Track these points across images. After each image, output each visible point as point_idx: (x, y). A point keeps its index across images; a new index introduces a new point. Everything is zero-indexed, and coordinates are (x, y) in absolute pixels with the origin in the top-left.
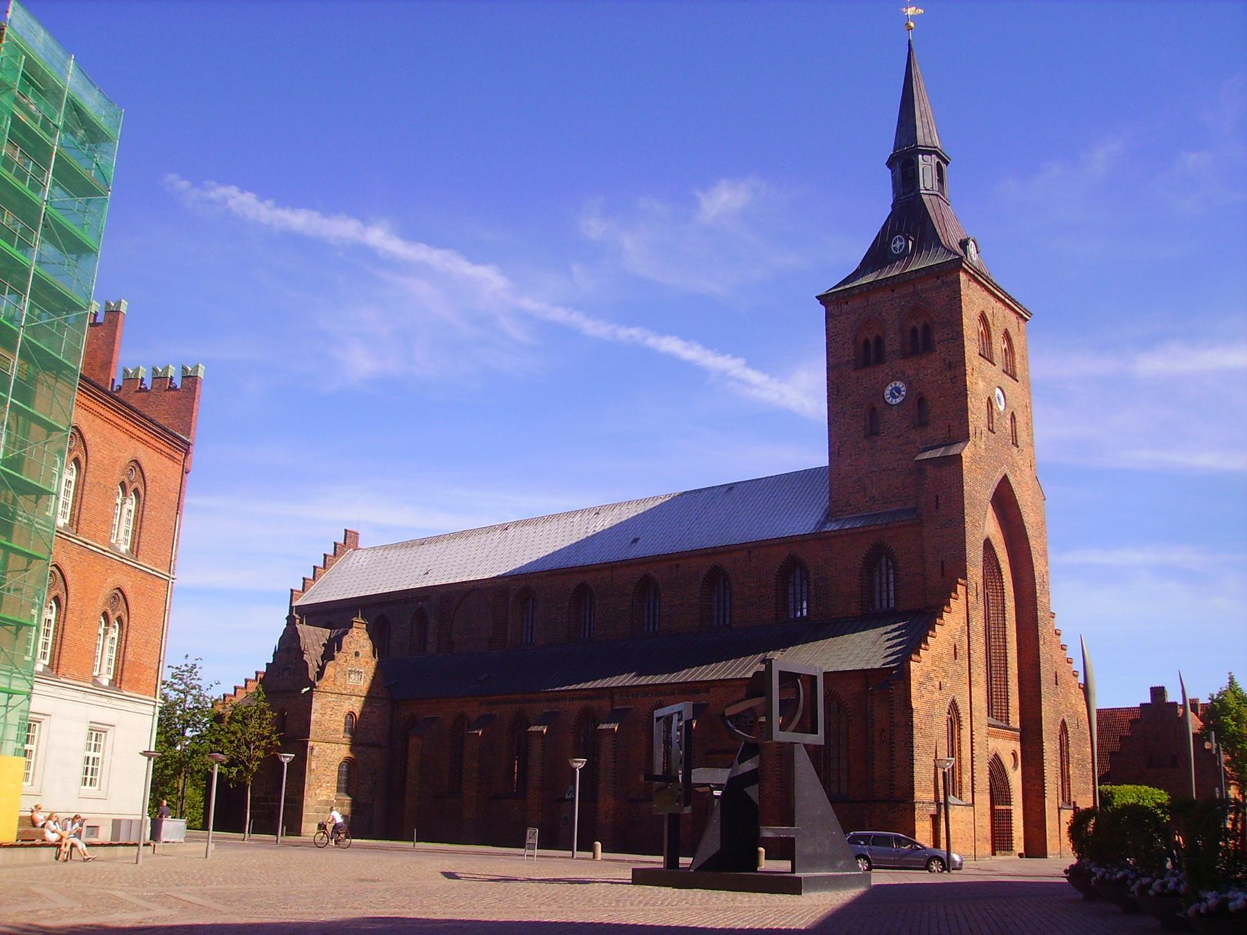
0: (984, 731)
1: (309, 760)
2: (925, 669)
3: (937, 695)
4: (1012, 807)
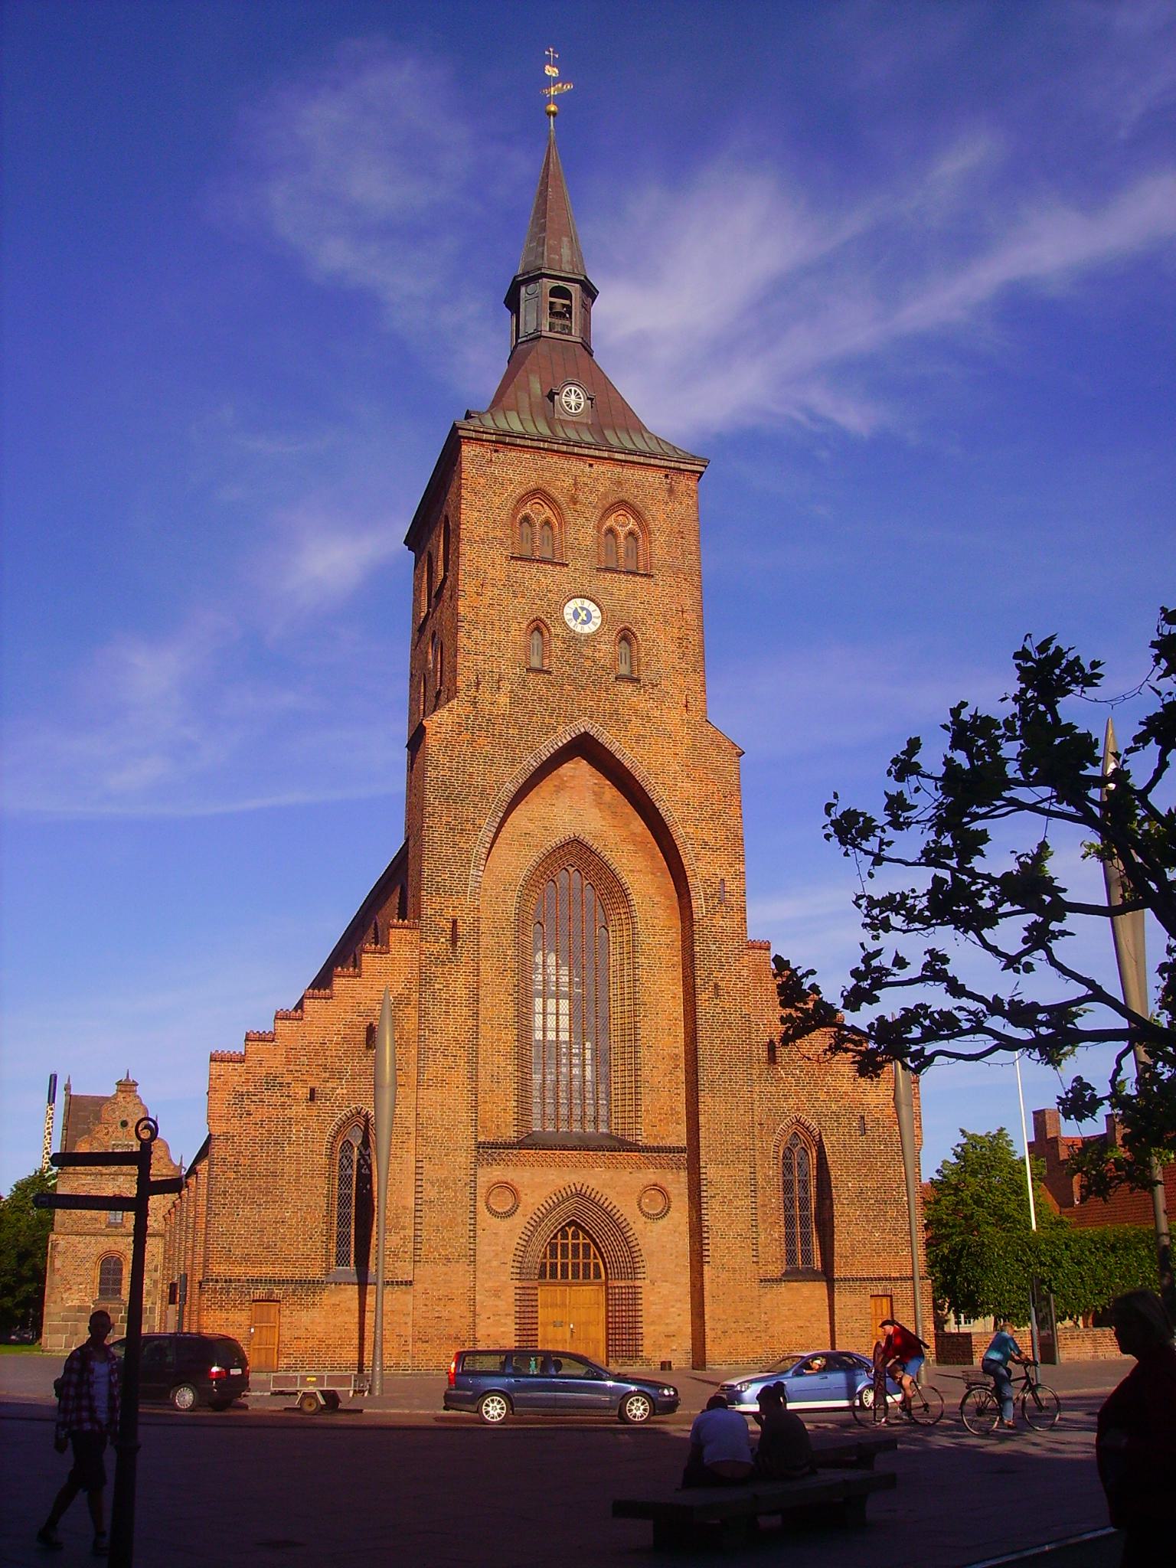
1: (51, 1257)
3: (299, 1110)
4: (638, 1283)
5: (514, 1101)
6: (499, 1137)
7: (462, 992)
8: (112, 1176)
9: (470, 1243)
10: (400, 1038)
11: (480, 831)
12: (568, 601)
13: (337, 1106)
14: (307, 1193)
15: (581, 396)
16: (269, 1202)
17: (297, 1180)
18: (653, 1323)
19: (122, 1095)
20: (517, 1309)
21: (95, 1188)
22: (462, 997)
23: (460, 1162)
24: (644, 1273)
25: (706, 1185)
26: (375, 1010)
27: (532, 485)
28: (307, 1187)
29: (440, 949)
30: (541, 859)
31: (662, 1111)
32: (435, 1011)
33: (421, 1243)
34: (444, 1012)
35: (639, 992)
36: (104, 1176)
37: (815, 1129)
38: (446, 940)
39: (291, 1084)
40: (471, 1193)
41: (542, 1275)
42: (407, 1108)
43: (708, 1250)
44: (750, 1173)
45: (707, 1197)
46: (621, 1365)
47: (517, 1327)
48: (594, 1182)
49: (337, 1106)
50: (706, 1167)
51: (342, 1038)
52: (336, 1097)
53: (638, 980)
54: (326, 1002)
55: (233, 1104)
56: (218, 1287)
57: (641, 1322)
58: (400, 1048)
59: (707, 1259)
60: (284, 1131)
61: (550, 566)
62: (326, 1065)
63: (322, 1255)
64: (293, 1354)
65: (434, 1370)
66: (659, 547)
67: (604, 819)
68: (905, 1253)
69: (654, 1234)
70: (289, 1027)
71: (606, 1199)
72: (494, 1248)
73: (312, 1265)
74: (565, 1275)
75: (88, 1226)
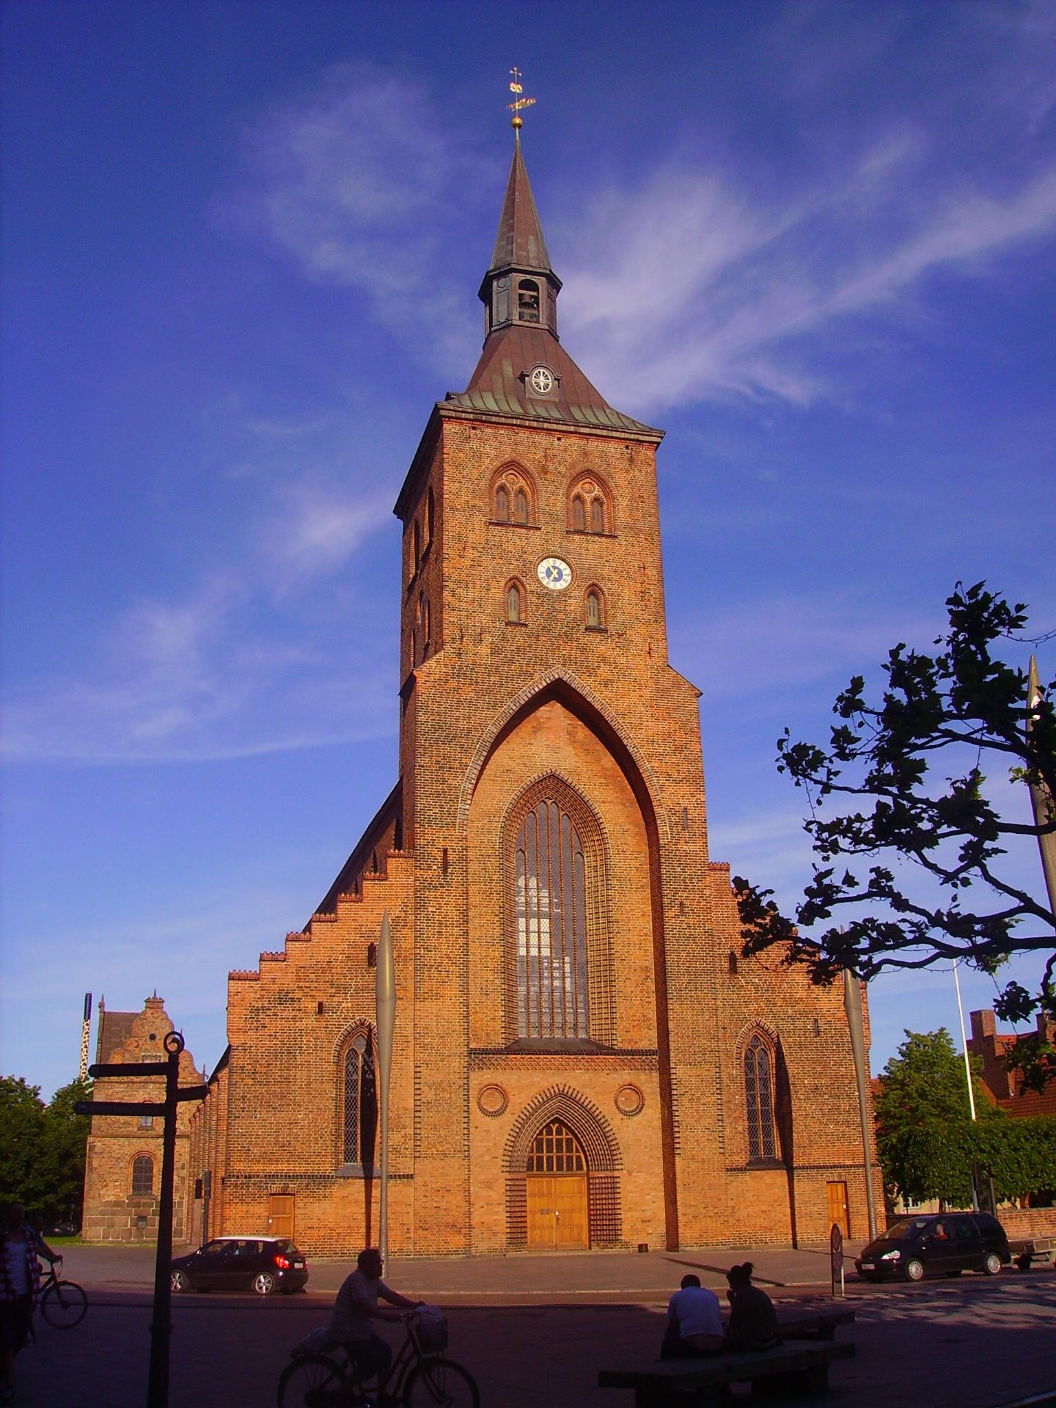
0: (457, 1064)
2: (276, 988)
3: (310, 1022)
4: (616, 1174)
6: (488, 1043)
7: (454, 914)
8: (142, 1084)
9: (464, 1140)
10: (398, 956)
11: (466, 769)
12: (542, 561)
13: (343, 1019)
14: (317, 1097)
15: (549, 377)
17: (309, 1083)
19: (150, 1011)
20: (508, 1198)
21: (127, 1095)
24: (622, 1164)
27: (507, 458)
28: (317, 1091)
29: (433, 875)
30: (521, 792)
32: (429, 932)
33: (420, 1140)
34: (437, 932)
35: (612, 911)
36: (135, 1085)
37: (773, 1032)
38: (438, 868)
39: (301, 999)
40: (464, 1095)
41: (530, 1168)
42: (406, 1018)
43: (679, 1143)
46: (603, 1248)
47: (508, 1215)
48: (575, 1083)
49: (343, 1019)
50: (676, 1068)
51: (346, 957)
52: (342, 1010)
53: (611, 900)
54: (332, 925)
55: (250, 1018)
56: (239, 1183)
57: (620, 1209)
58: (399, 965)
61: (524, 530)
62: (332, 982)
63: (332, 1152)
64: (307, 1242)
65: (434, 1255)
66: (622, 511)
67: (578, 756)
68: (857, 1143)
69: (630, 1129)
70: (298, 948)
71: (586, 1098)
72: (486, 1144)
74: (550, 1168)
75: (122, 1130)
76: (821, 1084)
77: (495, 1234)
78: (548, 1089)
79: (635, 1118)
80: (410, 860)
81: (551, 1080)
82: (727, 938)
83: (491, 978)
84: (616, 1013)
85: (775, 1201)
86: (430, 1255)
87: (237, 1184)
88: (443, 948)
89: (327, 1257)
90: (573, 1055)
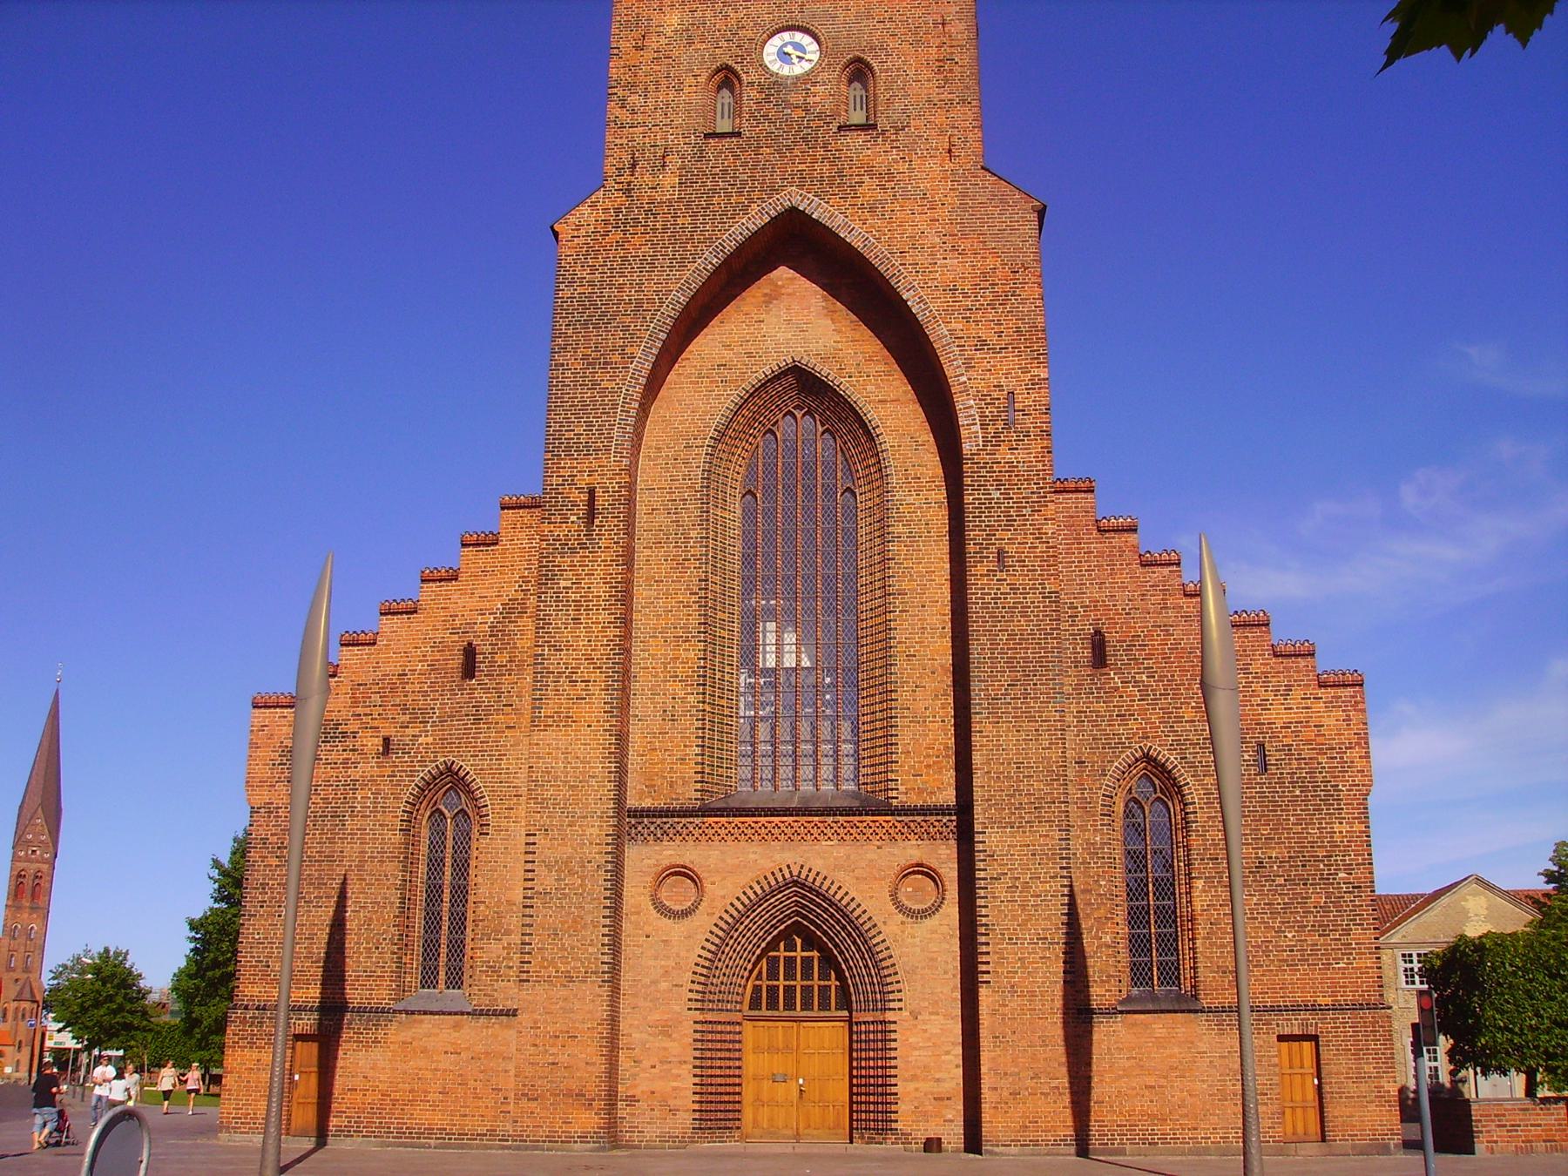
0: (595, 831)
4: (890, 1016)
5: (697, 746)
7: (600, 590)
9: (602, 954)
10: (511, 661)
11: (631, 363)
12: (770, 37)
13: (418, 761)
14: (373, 884)
16: (321, 898)
18: (914, 1078)
20: (698, 1054)
22: (600, 596)
23: (591, 834)
24: (900, 1000)
25: (985, 860)
26: (476, 623)
29: (570, 531)
30: (742, 398)
31: (931, 752)
32: (559, 619)
37: (1176, 766)
40: (605, 880)
41: (755, 1004)
43: (988, 963)
44: (1060, 840)
45: (986, 879)
46: (867, 1143)
47: (697, 1080)
48: (820, 862)
49: (418, 761)
52: (418, 748)
53: (894, 559)
57: (896, 1076)
58: (510, 675)
59: (985, 977)
60: (345, 798)
63: (391, 972)
64: (345, 1112)
65: (544, 1141)
67: (839, 332)
68: (1341, 965)
71: (840, 888)
72: (663, 963)
73: (376, 985)
74: (790, 1005)
76: (1270, 858)
77: (674, 1111)
78: (773, 874)
79: (928, 922)
80: (536, 510)
81: (777, 857)
82: (1087, 606)
83: (681, 694)
84: (897, 744)
85: (1172, 1068)
86: (538, 1141)
87: (245, 1018)
88: (581, 643)
89: (375, 1137)
90: (817, 815)
